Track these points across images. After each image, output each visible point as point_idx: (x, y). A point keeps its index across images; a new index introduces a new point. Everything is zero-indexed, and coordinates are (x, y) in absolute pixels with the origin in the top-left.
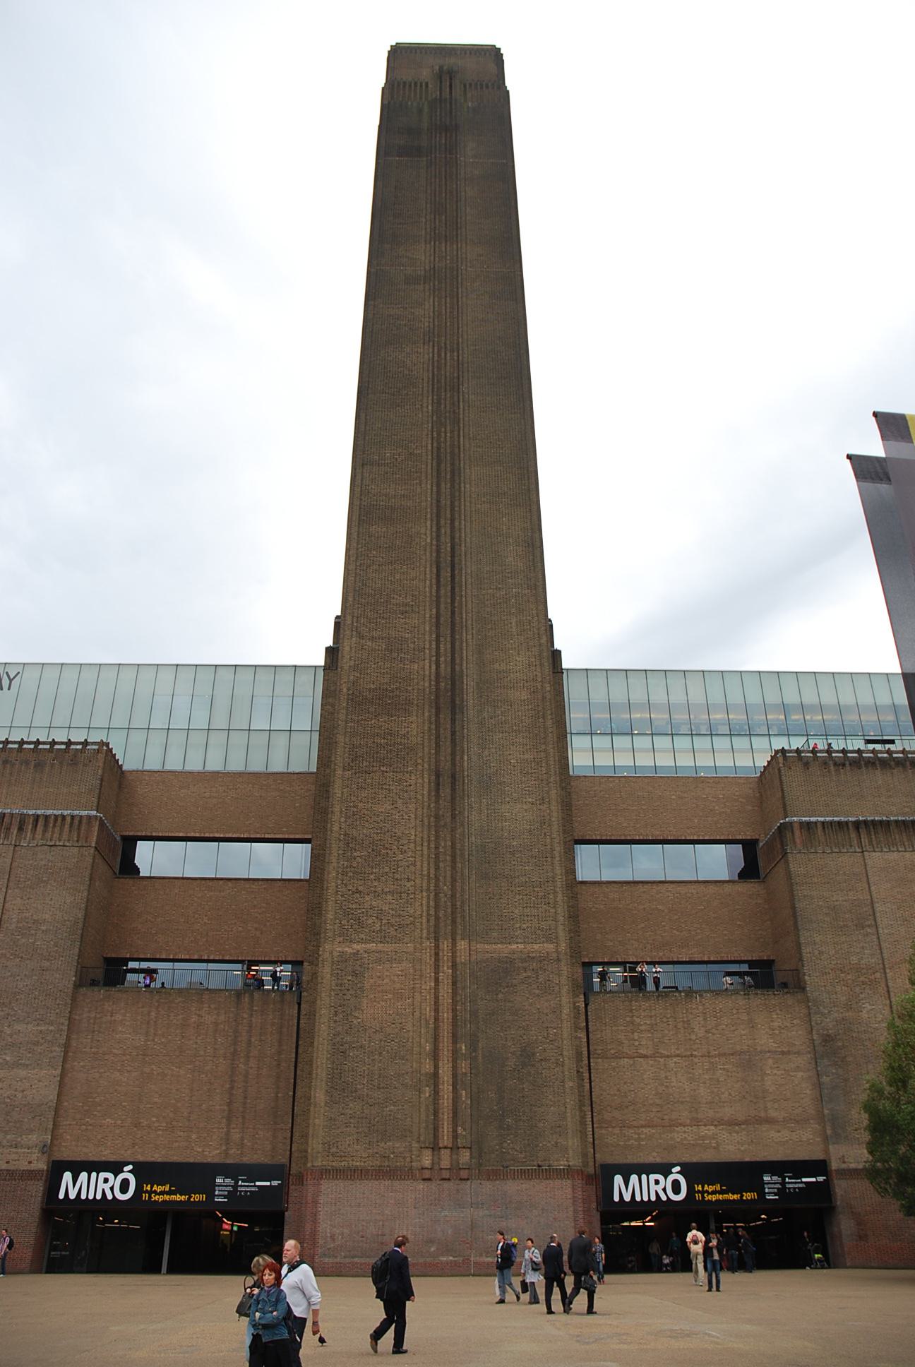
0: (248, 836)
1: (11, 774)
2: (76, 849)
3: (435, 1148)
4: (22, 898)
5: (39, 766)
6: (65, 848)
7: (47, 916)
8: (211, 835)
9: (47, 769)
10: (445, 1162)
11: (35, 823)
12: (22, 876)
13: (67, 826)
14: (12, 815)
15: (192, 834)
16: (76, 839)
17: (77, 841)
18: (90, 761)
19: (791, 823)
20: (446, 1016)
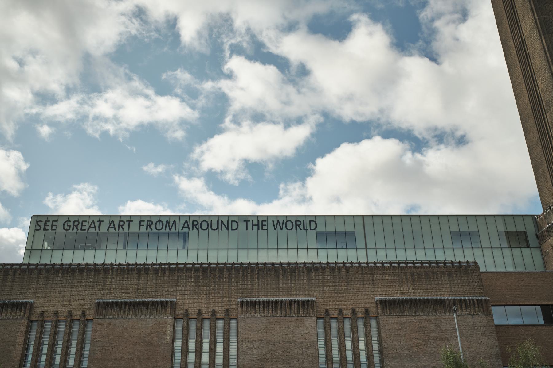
0: (536, 304)
1: (438, 279)
2: (484, 317)
4: (467, 341)
5: (450, 275)
6: (479, 316)
7: (482, 350)
8: (518, 304)
9: (454, 276)
11: (460, 304)
12: (463, 330)
13: (476, 306)
14: (449, 300)
15: (509, 303)
16: (482, 311)
17: (484, 312)
18: (474, 272)
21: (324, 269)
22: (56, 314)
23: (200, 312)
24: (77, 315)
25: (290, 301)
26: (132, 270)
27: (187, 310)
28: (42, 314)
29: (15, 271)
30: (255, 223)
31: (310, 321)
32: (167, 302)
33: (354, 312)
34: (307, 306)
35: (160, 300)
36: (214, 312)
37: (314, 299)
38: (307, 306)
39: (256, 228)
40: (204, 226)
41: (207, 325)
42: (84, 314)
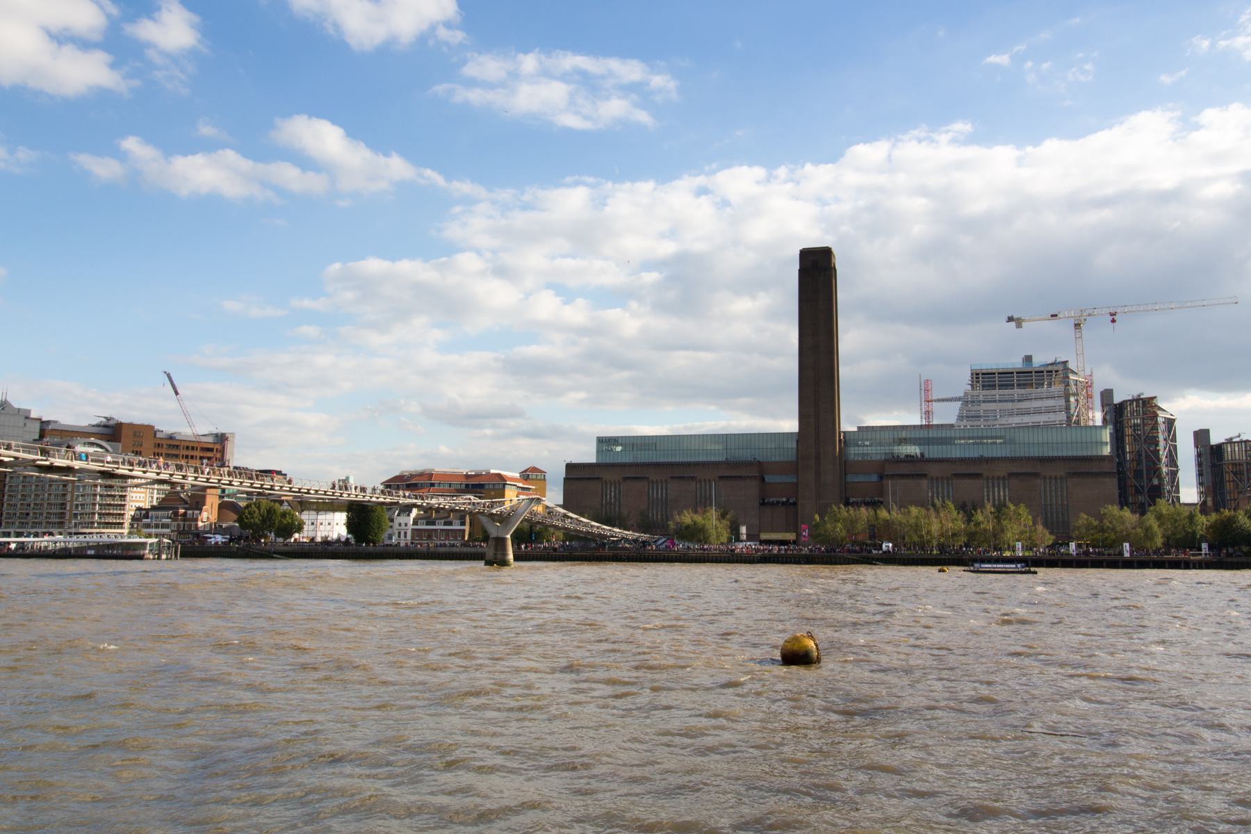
24: (617, 481)
31: (694, 484)
34: (693, 478)
38: (693, 478)
41: (660, 485)
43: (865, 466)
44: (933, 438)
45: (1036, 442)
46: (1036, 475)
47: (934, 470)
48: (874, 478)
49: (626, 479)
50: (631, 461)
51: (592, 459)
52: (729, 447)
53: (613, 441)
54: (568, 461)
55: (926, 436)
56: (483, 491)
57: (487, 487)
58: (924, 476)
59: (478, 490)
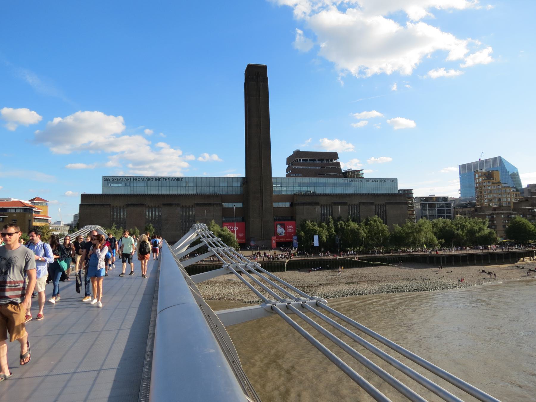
3: (262, 238)
10: (262, 239)
19: (296, 203)
20: (262, 226)
21: (182, 195)
22: (117, 207)
23: (152, 206)
25: (174, 204)
26: (134, 196)
27: (149, 206)
28: (113, 206)
29: (105, 196)
30: (166, 179)
32: (144, 204)
33: (189, 206)
34: (178, 205)
35: (142, 203)
36: (155, 206)
37: (180, 203)
39: (166, 180)
40: (152, 180)
42: (123, 206)
43: (283, 198)
44: (317, 183)
45: (364, 186)
46: (372, 204)
47: (323, 201)
48: (288, 205)
49: (128, 205)
50: (129, 193)
51: (100, 192)
52: (197, 185)
53: (116, 180)
54: (83, 193)
55: (313, 182)
56: (5, 213)
57: (9, 211)
58: (317, 204)
59: (2, 213)
